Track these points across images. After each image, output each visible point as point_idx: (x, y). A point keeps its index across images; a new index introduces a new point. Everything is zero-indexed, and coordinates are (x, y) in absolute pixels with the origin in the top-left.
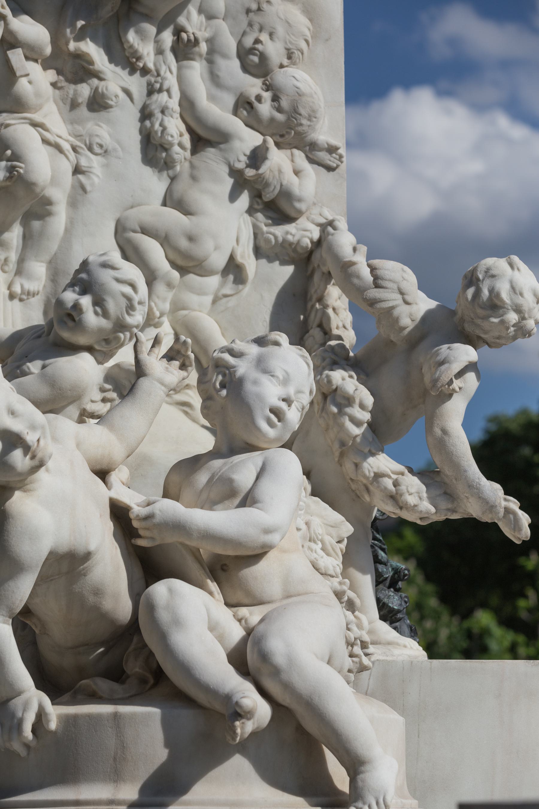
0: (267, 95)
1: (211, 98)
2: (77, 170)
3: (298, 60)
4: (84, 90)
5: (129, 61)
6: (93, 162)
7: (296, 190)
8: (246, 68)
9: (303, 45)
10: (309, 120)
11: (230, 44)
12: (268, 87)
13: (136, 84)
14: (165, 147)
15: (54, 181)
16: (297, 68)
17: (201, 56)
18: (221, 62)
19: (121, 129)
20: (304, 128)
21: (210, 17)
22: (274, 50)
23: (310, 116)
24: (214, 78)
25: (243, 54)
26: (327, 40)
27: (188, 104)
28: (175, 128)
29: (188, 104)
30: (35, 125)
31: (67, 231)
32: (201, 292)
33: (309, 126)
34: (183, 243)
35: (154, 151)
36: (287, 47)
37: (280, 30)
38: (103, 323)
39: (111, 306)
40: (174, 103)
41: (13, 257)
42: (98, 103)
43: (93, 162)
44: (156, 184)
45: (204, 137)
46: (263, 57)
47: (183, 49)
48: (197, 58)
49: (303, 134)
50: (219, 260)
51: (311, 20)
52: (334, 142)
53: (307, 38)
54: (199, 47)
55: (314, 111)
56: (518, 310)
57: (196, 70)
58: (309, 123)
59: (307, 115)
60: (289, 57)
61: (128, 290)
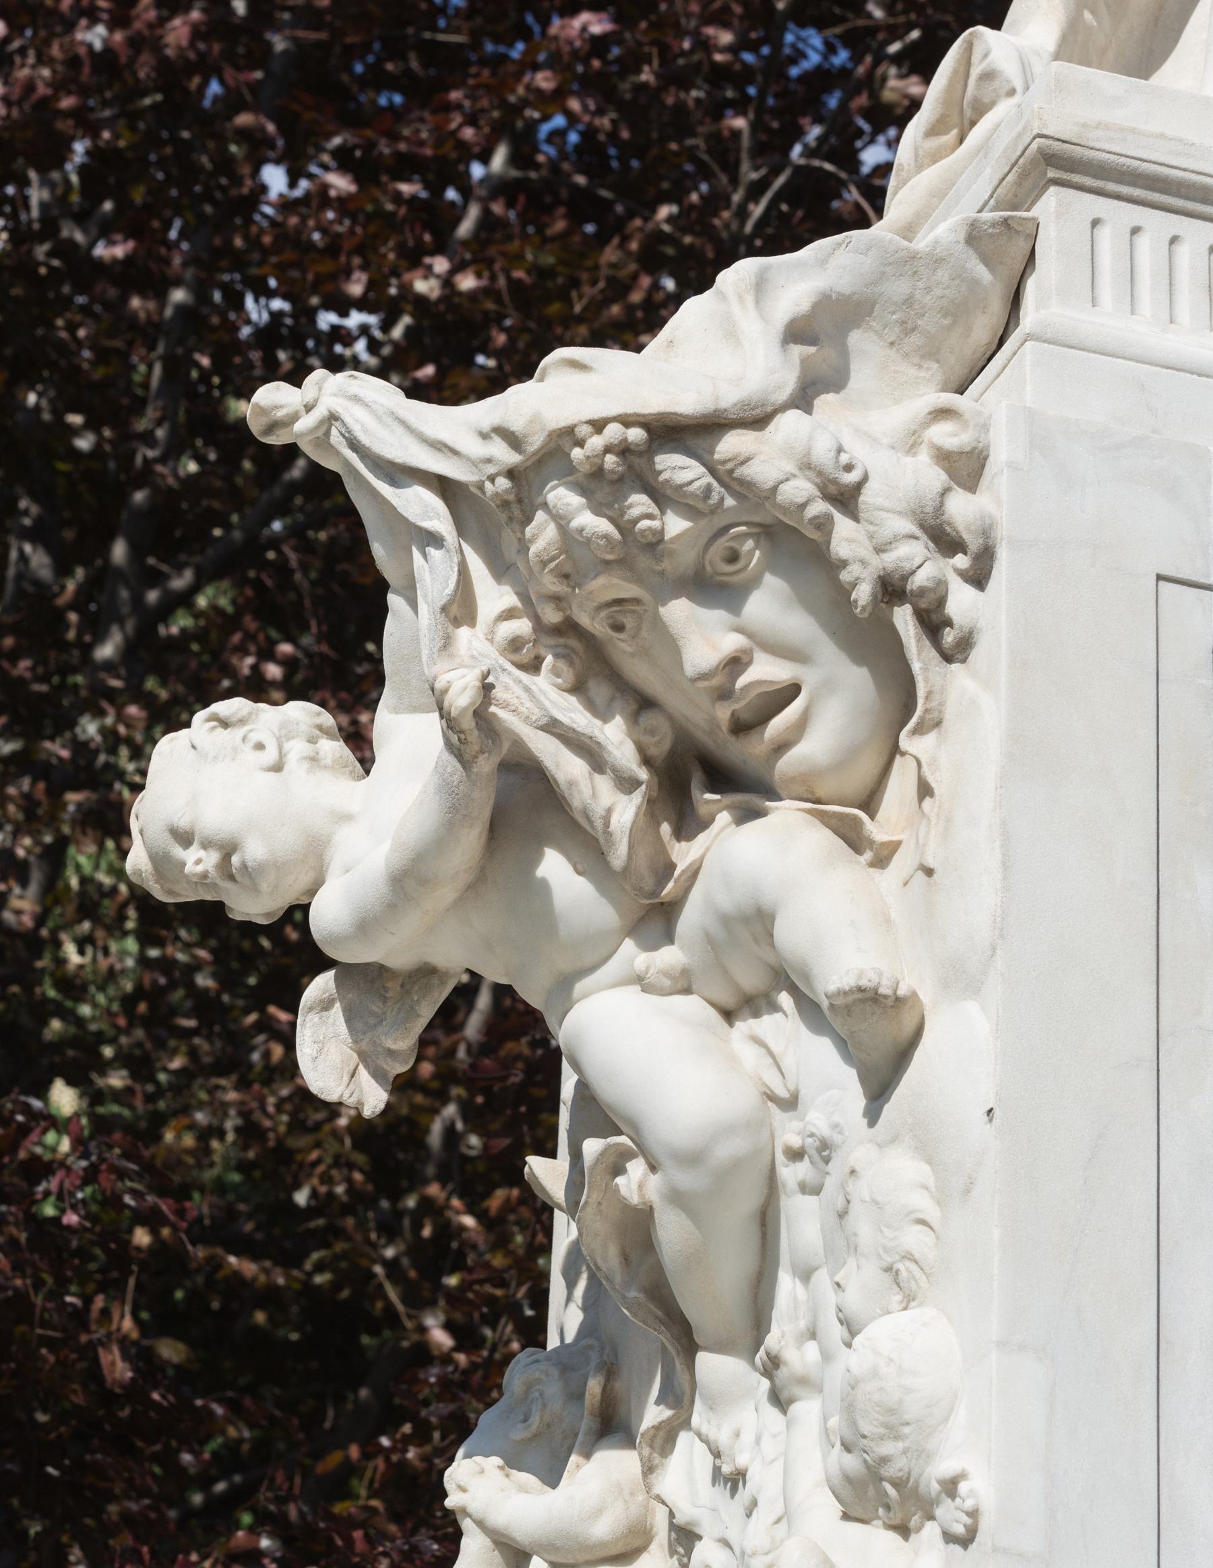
3: (913, 1286)
10: (897, 1438)
16: (921, 1305)
20: (899, 1465)
23: (889, 1427)
26: (967, 1191)
33: (905, 1452)
36: (885, 1265)
48: (797, 1391)
49: (908, 1479)
51: (929, 1162)
53: (921, 1216)
54: (786, 1364)
55: (891, 1411)
58: (900, 1445)
59: (882, 1430)
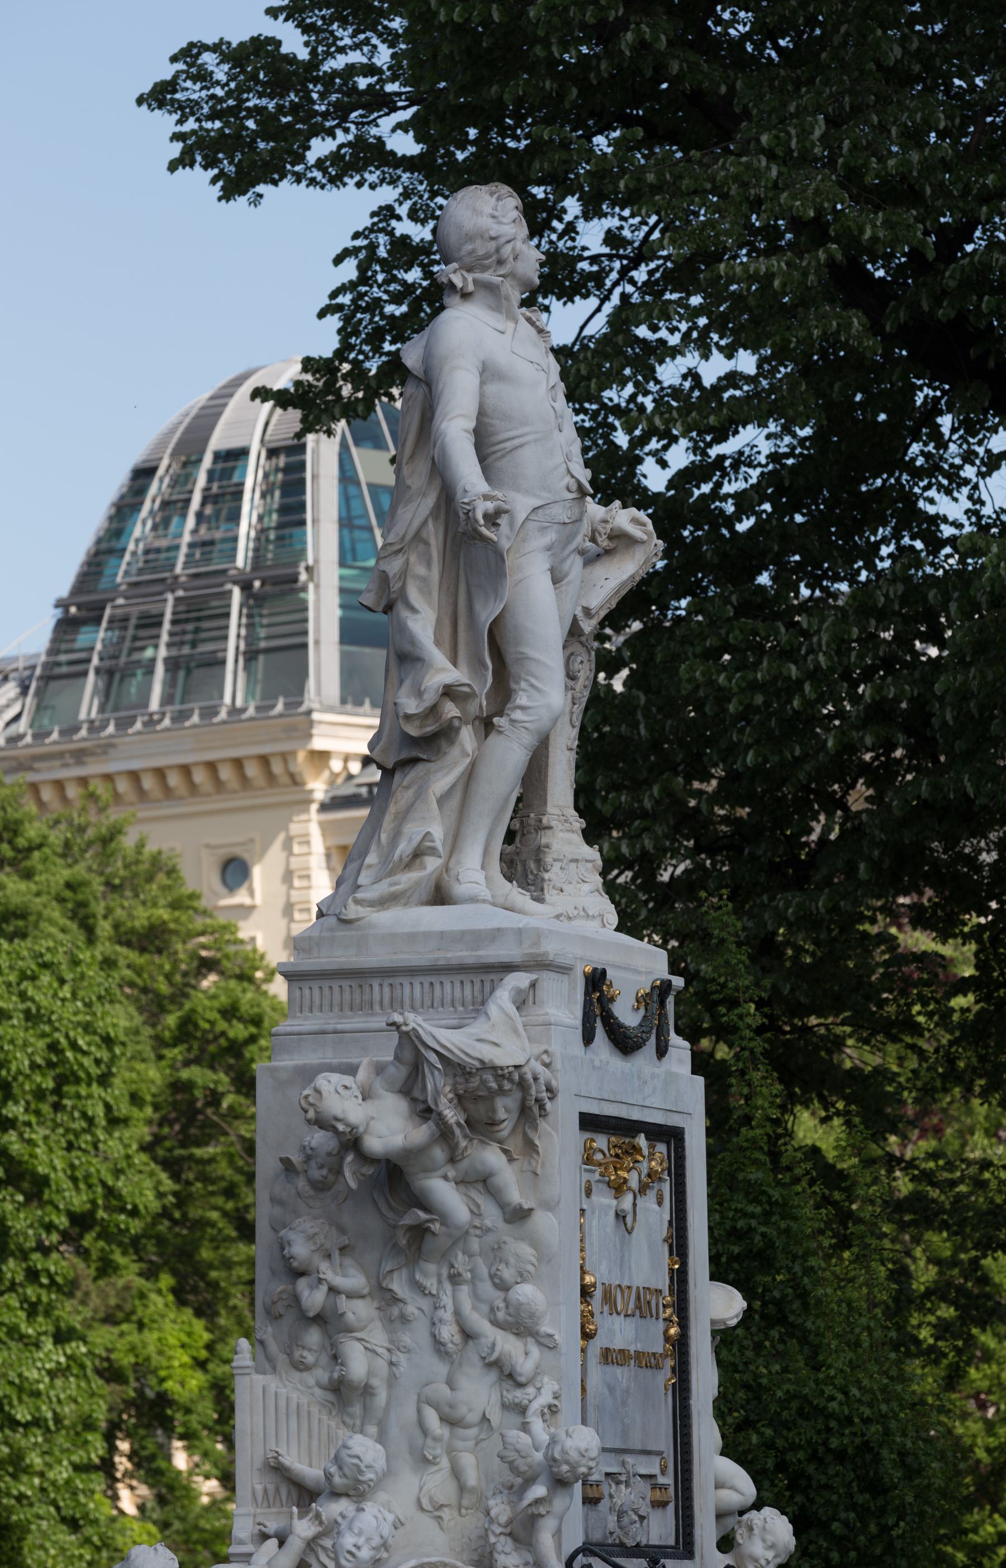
0: (502, 1305)
1: (474, 1308)
2: (391, 1364)
4: (396, 1311)
5: (421, 1289)
6: (401, 1358)
7: (518, 1369)
8: (496, 1286)
9: (530, 1268)
11: (484, 1271)
12: (505, 1300)
13: (425, 1304)
14: (444, 1345)
15: (370, 1373)
17: (466, 1282)
18: (479, 1285)
19: (417, 1336)
21: (471, 1256)
22: (508, 1274)
24: (475, 1296)
25: (492, 1277)
27: (457, 1313)
28: (448, 1332)
29: (457, 1313)
30: (360, 1340)
31: (388, 1403)
32: (465, 1439)
34: (447, 1410)
35: (438, 1346)
37: (512, 1260)
38: (345, 1481)
39: (346, 1471)
40: (448, 1315)
41: (358, 1422)
42: (404, 1319)
43: (401, 1358)
44: (442, 1369)
45: (468, 1335)
46: (501, 1279)
47: (455, 1279)
50: (473, 1417)
52: (550, 1331)
56: (567, 1463)
57: (465, 1290)
60: (521, 1275)
61: (356, 1461)
